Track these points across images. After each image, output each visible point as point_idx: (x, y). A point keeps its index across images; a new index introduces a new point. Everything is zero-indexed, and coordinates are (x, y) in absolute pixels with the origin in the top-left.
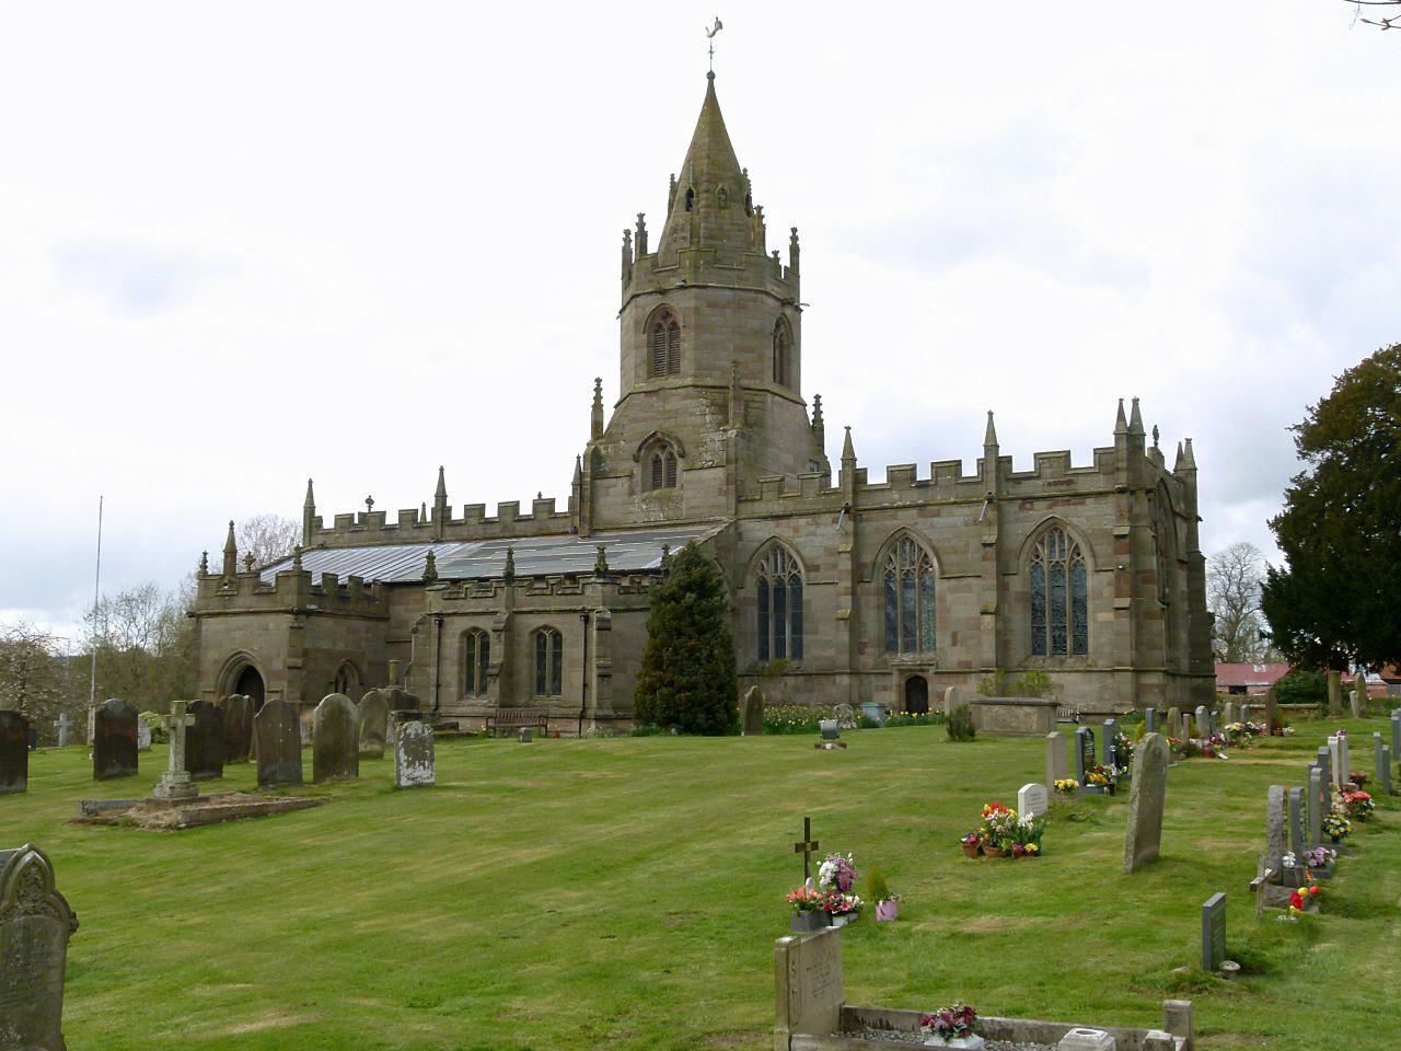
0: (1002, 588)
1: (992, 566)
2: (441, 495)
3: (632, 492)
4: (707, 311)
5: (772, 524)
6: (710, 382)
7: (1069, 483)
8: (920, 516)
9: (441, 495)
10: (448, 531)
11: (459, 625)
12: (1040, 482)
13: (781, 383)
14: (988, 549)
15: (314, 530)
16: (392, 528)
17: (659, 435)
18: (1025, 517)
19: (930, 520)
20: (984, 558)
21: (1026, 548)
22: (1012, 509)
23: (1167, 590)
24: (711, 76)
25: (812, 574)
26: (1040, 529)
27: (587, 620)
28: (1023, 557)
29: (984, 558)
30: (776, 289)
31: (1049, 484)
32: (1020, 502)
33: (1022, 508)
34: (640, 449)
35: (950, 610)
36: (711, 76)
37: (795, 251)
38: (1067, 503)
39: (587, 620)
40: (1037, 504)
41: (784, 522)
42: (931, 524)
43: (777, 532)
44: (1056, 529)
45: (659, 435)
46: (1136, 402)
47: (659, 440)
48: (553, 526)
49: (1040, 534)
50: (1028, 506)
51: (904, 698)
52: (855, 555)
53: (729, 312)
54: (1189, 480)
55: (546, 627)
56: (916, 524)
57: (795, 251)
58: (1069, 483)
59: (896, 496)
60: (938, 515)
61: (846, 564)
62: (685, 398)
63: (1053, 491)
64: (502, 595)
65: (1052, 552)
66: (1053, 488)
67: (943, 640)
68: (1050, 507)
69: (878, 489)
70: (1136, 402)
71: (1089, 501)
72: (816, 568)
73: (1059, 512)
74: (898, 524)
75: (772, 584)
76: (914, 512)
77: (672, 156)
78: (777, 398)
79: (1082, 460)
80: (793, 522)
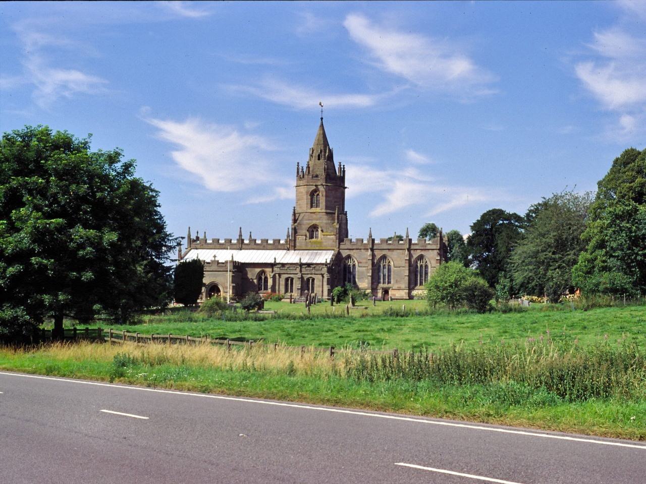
6: (328, 211)
10: (244, 246)
11: (284, 277)
15: (192, 243)
16: (222, 244)
22: (412, 252)
25: (360, 264)
27: (323, 277)
29: (406, 263)
39: (323, 277)
41: (351, 251)
48: (279, 247)
55: (311, 277)
64: (298, 270)
65: (420, 262)
69: (378, 244)
71: (430, 251)
72: (361, 263)
73: (423, 253)
77: (310, 141)
80: (354, 251)
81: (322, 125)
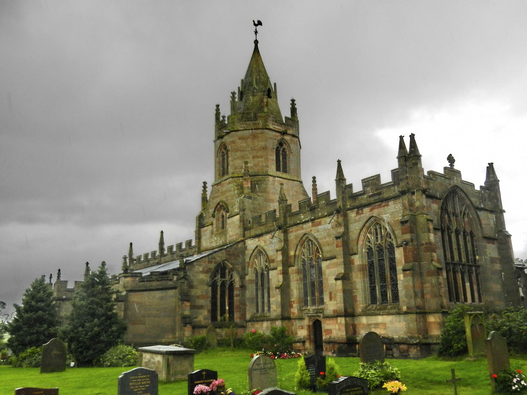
0: (348, 264)
1: (340, 251)
2: (162, 243)
3: (212, 233)
4: (238, 141)
5: (257, 239)
7: (379, 194)
8: (313, 226)
9: (162, 243)
12: (365, 196)
13: (285, 171)
14: (338, 240)
17: (221, 203)
18: (360, 218)
19: (317, 228)
20: (337, 246)
21: (362, 237)
23: (477, 257)
24: (256, 42)
26: (367, 225)
28: (360, 243)
29: (337, 246)
30: (276, 127)
31: (370, 197)
32: (356, 210)
33: (357, 213)
34: (214, 212)
35: (327, 279)
36: (256, 42)
37: (294, 110)
38: (380, 206)
40: (366, 210)
42: (317, 230)
43: (258, 243)
44: (377, 224)
45: (221, 203)
46: (412, 136)
47: (221, 206)
49: (369, 227)
50: (360, 212)
51: (312, 333)
52: (284, 251)
53: (249, 141)
54: (455, 181)
56: (311, 230)
57: (294, 110)
58: (379, 194)
59: (302, 217)
60: (320, 224)
61: (280, 258)
62: (229, 183)
63: (372, 199)
66: (372, 199)
67: (326, 299)
68: (371, 210)
70: (412, 136)
71: (391, 203)
73: (375, 212)
74: (303, 231)
75: (259, 271)
76: (310, 224)
78: (276, 178)
79: (386, 178)
81: (256, 50)
